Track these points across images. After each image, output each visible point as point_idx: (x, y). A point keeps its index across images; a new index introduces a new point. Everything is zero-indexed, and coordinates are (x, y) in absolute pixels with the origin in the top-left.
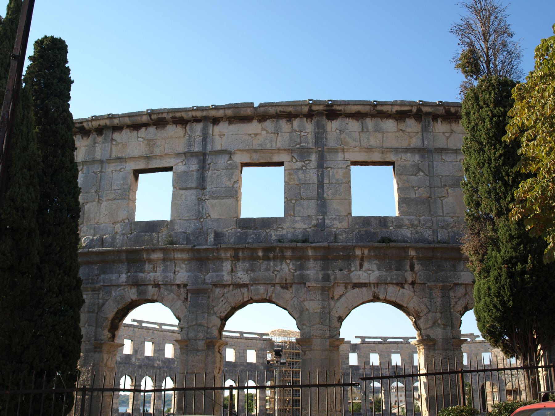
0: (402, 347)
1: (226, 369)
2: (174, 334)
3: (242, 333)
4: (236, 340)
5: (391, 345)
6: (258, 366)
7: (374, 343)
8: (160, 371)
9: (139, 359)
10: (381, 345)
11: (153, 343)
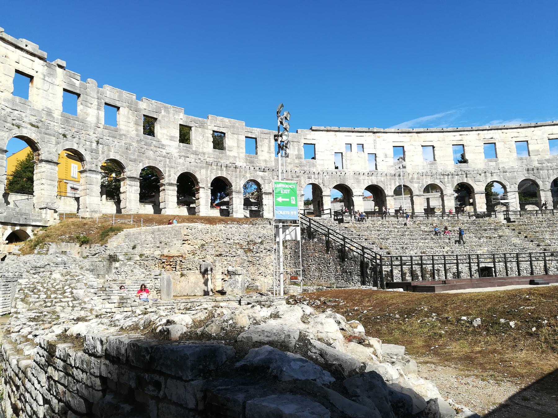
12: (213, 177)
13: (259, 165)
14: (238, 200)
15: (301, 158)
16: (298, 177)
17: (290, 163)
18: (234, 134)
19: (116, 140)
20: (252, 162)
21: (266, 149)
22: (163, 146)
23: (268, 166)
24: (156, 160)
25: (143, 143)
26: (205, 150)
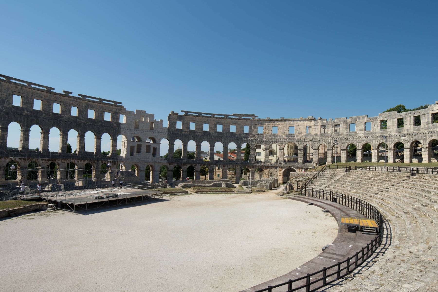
0: (210, 120)
1: (88, 123)
2: (43, 93)
3: (101, 100)
4: (97, 104)
5: (204, 118)
6: (112, 123)
7: (193, 116)
8: (28, 119)
9: (6, 108)
10: (198, 118)
11: (22, 97)
12: (378, 143)
13: (404, 133)
14: (390, 153)
15: (429, 124)
16: (425, 136)
17: (422, 128)
18: (391, 119)
19: (338, 137)
20: (400, 132)
21: (408, 123)
22: (357, 134)
23: (409, 132)
24: (353, 141)
25: (349, 135)
26: (377, 131)
